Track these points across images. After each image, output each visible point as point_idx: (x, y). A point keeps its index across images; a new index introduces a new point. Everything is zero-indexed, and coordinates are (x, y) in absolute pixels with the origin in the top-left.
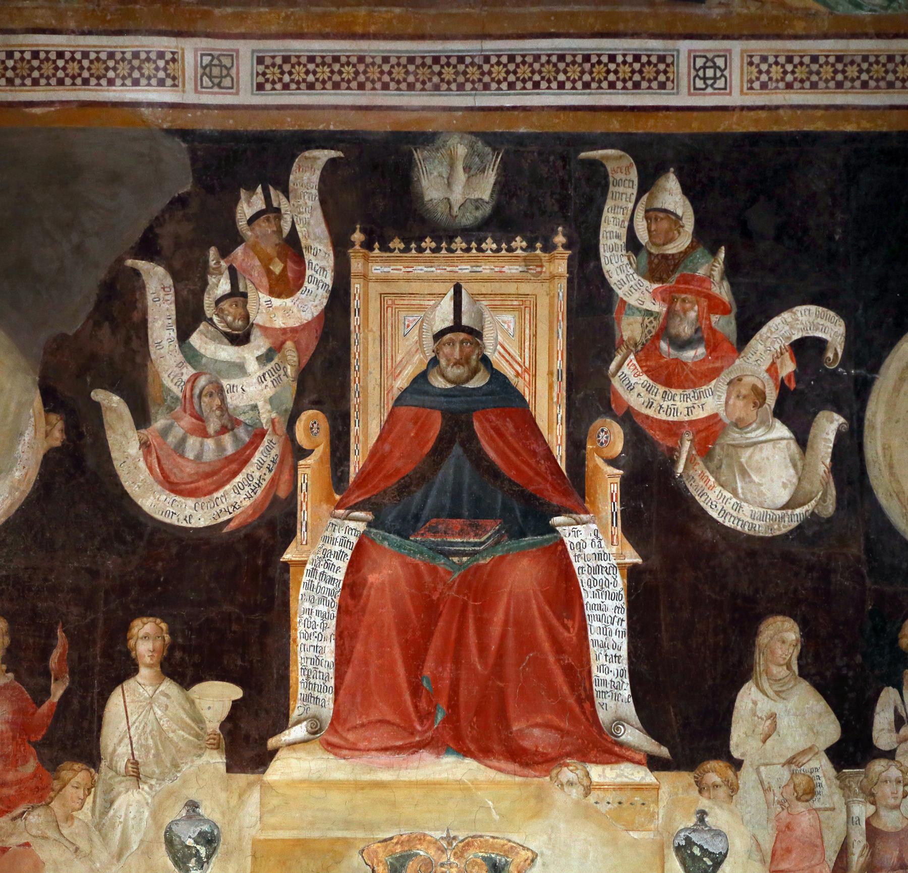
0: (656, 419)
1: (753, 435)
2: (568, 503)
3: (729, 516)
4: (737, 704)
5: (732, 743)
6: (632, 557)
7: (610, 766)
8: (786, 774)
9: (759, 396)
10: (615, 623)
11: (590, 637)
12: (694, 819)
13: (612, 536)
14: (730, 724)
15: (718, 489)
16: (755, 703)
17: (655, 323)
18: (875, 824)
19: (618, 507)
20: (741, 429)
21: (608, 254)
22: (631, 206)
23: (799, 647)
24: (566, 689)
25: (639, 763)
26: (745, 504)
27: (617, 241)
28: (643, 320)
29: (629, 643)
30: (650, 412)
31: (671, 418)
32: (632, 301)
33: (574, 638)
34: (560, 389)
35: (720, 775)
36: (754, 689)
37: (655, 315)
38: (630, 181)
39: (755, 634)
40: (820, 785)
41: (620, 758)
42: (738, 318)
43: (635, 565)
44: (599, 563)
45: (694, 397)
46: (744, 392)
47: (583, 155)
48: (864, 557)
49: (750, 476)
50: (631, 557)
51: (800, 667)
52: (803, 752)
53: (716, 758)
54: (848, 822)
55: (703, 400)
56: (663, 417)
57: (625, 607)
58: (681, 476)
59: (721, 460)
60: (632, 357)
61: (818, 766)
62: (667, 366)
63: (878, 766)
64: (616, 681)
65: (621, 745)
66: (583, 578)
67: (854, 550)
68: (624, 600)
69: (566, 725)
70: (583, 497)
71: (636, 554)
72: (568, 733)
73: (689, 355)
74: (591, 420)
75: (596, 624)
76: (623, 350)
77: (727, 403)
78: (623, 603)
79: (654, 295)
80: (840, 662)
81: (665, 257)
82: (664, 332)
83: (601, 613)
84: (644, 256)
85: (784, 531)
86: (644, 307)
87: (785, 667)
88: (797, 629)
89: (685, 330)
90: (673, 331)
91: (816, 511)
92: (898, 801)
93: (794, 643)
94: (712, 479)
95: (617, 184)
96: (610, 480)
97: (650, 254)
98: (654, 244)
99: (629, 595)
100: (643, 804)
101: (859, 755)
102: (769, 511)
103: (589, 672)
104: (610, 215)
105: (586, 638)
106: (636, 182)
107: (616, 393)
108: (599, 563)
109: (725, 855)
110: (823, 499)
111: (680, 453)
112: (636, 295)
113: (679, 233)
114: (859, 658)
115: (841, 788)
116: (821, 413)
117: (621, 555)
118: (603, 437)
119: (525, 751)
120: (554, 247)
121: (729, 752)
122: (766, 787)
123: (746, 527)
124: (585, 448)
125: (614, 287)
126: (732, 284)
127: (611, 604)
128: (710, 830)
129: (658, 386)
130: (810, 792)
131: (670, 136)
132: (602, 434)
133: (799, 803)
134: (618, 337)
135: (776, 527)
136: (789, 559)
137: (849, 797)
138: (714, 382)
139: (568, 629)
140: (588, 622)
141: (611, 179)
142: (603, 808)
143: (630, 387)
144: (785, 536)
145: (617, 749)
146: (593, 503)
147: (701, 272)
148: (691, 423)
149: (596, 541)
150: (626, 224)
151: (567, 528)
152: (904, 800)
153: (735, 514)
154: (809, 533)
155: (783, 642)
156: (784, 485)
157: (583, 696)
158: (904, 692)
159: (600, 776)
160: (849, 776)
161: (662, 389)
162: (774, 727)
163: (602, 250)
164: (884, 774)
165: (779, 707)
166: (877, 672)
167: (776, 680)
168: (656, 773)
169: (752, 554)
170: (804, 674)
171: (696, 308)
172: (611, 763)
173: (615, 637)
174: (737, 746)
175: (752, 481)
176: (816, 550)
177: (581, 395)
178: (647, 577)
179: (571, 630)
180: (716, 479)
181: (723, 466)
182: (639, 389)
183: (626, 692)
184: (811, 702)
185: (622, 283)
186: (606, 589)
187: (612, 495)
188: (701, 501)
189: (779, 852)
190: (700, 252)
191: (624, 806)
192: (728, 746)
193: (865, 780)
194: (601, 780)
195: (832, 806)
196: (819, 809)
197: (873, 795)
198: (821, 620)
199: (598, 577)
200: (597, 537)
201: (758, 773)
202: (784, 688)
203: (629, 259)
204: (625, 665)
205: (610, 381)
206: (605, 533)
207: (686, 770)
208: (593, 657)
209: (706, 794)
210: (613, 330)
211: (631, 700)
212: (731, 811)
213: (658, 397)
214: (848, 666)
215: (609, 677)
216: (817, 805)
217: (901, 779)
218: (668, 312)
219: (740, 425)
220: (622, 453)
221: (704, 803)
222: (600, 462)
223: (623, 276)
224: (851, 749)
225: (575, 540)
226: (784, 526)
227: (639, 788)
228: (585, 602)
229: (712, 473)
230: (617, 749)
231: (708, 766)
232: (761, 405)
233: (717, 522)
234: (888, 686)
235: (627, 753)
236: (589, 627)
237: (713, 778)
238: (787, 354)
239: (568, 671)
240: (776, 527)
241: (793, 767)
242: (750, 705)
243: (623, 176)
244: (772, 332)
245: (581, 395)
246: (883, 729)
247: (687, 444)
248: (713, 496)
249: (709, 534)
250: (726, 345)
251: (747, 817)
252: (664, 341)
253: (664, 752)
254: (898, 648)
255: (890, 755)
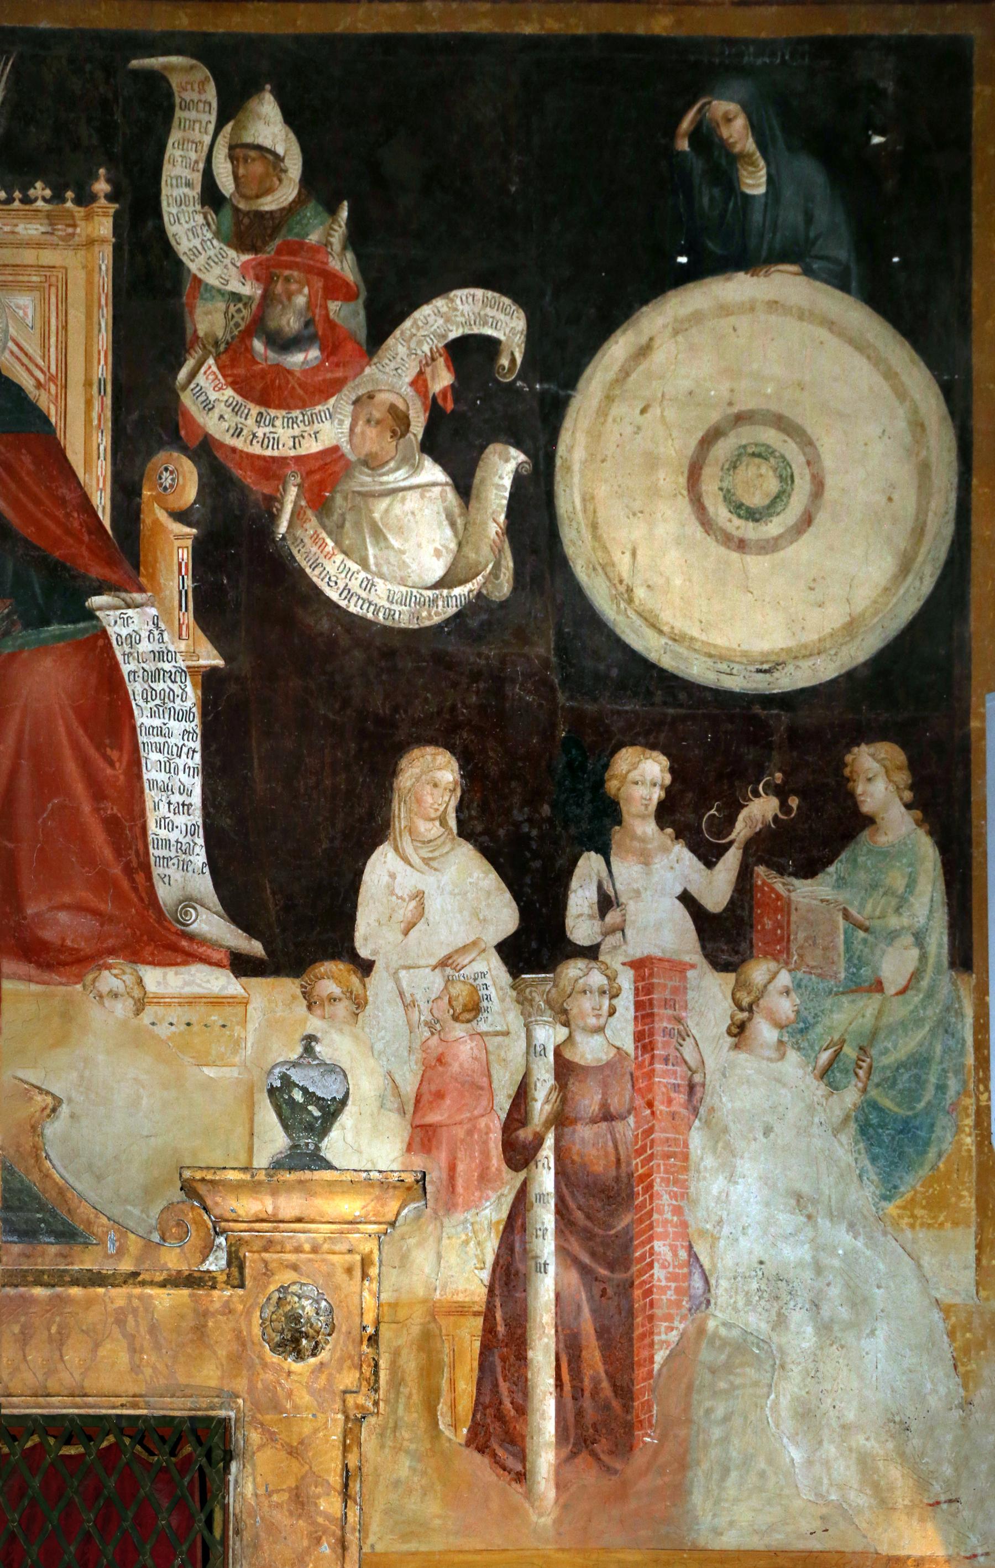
0: (247, 454)
1: (390, 478)
2: (113, 576)
3: (354, 599)
4: (366, 877)
5: (357, 934)
6: (210, 658)
7: (174, 969)
8: (436, 981)
9: (400, 421)
10: (184, 756)
11: (146, 776)
12: (300, 1050)
13: (180, 626)
14: (355, 907)
15: (339, 557)
16: (393, 876)
17: (245, 312)
18: (568, 1055)
19: (189, 583)
20: (373, 469)
21: (174, 210)
22: (207, 139)
23: (459, 793)
24: (108, 853)
25: (218, 965)
26: (380, 583)
27: (186, 190)
28: (228, 308)
29: (204, 786)
30: (238, 443)
31: (269, 453)
32: (211, 279)
33: (122, 778)
34: (103, 407)
35: (339, 982)
36: (391, 854)
37: (245, 300)
38: (205, 102)
39: (393, 773)
40: (488, 998)
41: (190, 958)
42: (368, 306)
43: (214, 670)
44: (160, 665)
45: (303, 421)
46: (377, 415)
47: (135, 63)
48: (554, 659)
49: (386, 539)
50: (208, 658)
51: (460, 822)
52: (464, 949)
53: (334, 957)
54: (528, 1053)
55: (317, 426)
56: (256, 449)
57: (198, 731)
58: (284, 538)
59: (343, 515)
60: (211, 361)
61: (485, 970)
62: (263, 374)
63: (573, 969)
64: (184, 841)
65: (191, 937)
66: (135, 688)
67: (542, 651)
68: (197, 721)
69: (108, 907)
70: (136, 566)
71: (215, 652)
72: (111, 919)
73: (296, 359)
74: (150, 454)
75: (155, 756)
76: (198, 353)
77: (352, 430)
78: (195, 725)
79: (244, 271)
80: (518, 816)
81: (260, 215)
82: (258, 325)
83: (162, 740)
84: (227, 212)
85: (436, 620)
86: (230, 288)
87: (437, 823)
88: (455, 765)
89: (291, 323)
90: (272, 325)
91: (484, 592)
92: (602, 1021)
93: (451, 786)
94: (330, 544)
95: (186, 107)
96: (177, 543)
97: (236, 210)
98: (243, 196)
99: (204, 714)
100: (224, 1026)
101: (545, 954)
102: (415, 591)
103: (144, 828)
104: (178, 153)
105: (139, 776)
106: (215, 105)
107: (186, 413)
108: (160, 665)
109: (344, 1102)
110: (495, 573)
111: (282, 504)
112: (217, 270)
113: (280, 180)
114: (546, 810)
115: (518, 1002)
116: (491, 448)
117: (192, 654)
118: (167, 479)
119: (44, 946)
120: (93, 198)
121: (353, 949)
122: (408, 999)
123: (381, 615)
124: (140, 495)
125: (184, 259)
126: (359, 257)
127: (176, 727)
128: (323, 1064)
129: (251, 405)
130: (473, 1009)
131: (263, 38)
132: (165, 475)
133: (457, 1025)
134: (189, 332)
135: (424, 614)
136: (442, 661)
137: (530, 1016)
138: (332, 401)
139: (112, 764)
140: (142, 753)
141: (177, 100)
142: (163, 1031)
143: (209, 407)
144: (439, 628)
145: (184, 943)
146: (152, 577)
147: (314, 238)
148: (299, 459)
149: (156, 632)
150: (201, 166)
151: (111, 613)
152: (611, 1019)
153: (364, 594)
154: (474, 623)
155: (436, 785)
156: (438, 553)
157: (135, 864)
158: (612, 859)
159: (159, 983)
160: (532, 984)
161: (255, 410)
162: (421, 912)
163: (164, 204)
164: (581, 981)
165: (428, 882)
166: (573, 830)
167: (424, 842)
168: (244, 979)
169: (389, 654)
170: (465, 832)
171: (306, 290)
172: (176, 964)
173: (183, 777)
174: (366, 939)
175: (389, 547)
176: (484, 650)
177: (135, 416)
178: (233, 688)
179: (117, 765)
180: (338, 543)
181: (347, 525)
182: (221, 408)
183: (200, 858)
184: (475, 875)
185: (195, 253)
186: (171, 705)
187: (180, 564)
188: (314, 575)
189: (426, 1098)
190: (311, 210)
191: (195, 1028)
192: (352, 939)
193: (554, 991)
194: (161, 990)
195: (505, 1028)
196: (487, 1034)
197: (565, 1012)
198: (491, 754)
199: (159, 686)
200: (157, 627)
201: (397, 981)
202: (436, 854)
203: (205, 218)
204: (197, 817)
205: (178, 396)
206: (169, 622)
207: (288, 975)
208: (149, 805)
209: (319, 1012)
210: (183, 322)
211: (206, 870)
212: (356, 1038)
213: (250, 422)
214: (530, 820)
215: (174, 836)
216: (483, 1027)
217: (606, 988)
218: (265, 296)
219: (372, 463)
220: (195, 502)
221: (314, 1024)
222: (162, 516)
223: (197, 242)
224: (534, 945)
225: (124, 632)
226: (437, 614)
227: (217, 1002)
228: (138, 724)
229: (330, 534)
230: (184, 943)
231: (322, 969)
232: (403, 435)
233: (338, 607)
234: (589, 850)
235: (201, 950)
236: (143, 761)
237: (329, 987)
238: (441, 361)
239: (112, 826)
240: (424, 614)
241: (448, 970)
242: (386, 879)
243: (195, 96)
244: (418, 328)
245: (135, 416)
246: (581, 915)
247: (293, 492)
248: (331, 568)
249: (325, 625)
250: (350, 346)
251: (379, 1046)
252: (258, 339)
253: (256, 948)
254: (605, 793)
255: (591, 953)
